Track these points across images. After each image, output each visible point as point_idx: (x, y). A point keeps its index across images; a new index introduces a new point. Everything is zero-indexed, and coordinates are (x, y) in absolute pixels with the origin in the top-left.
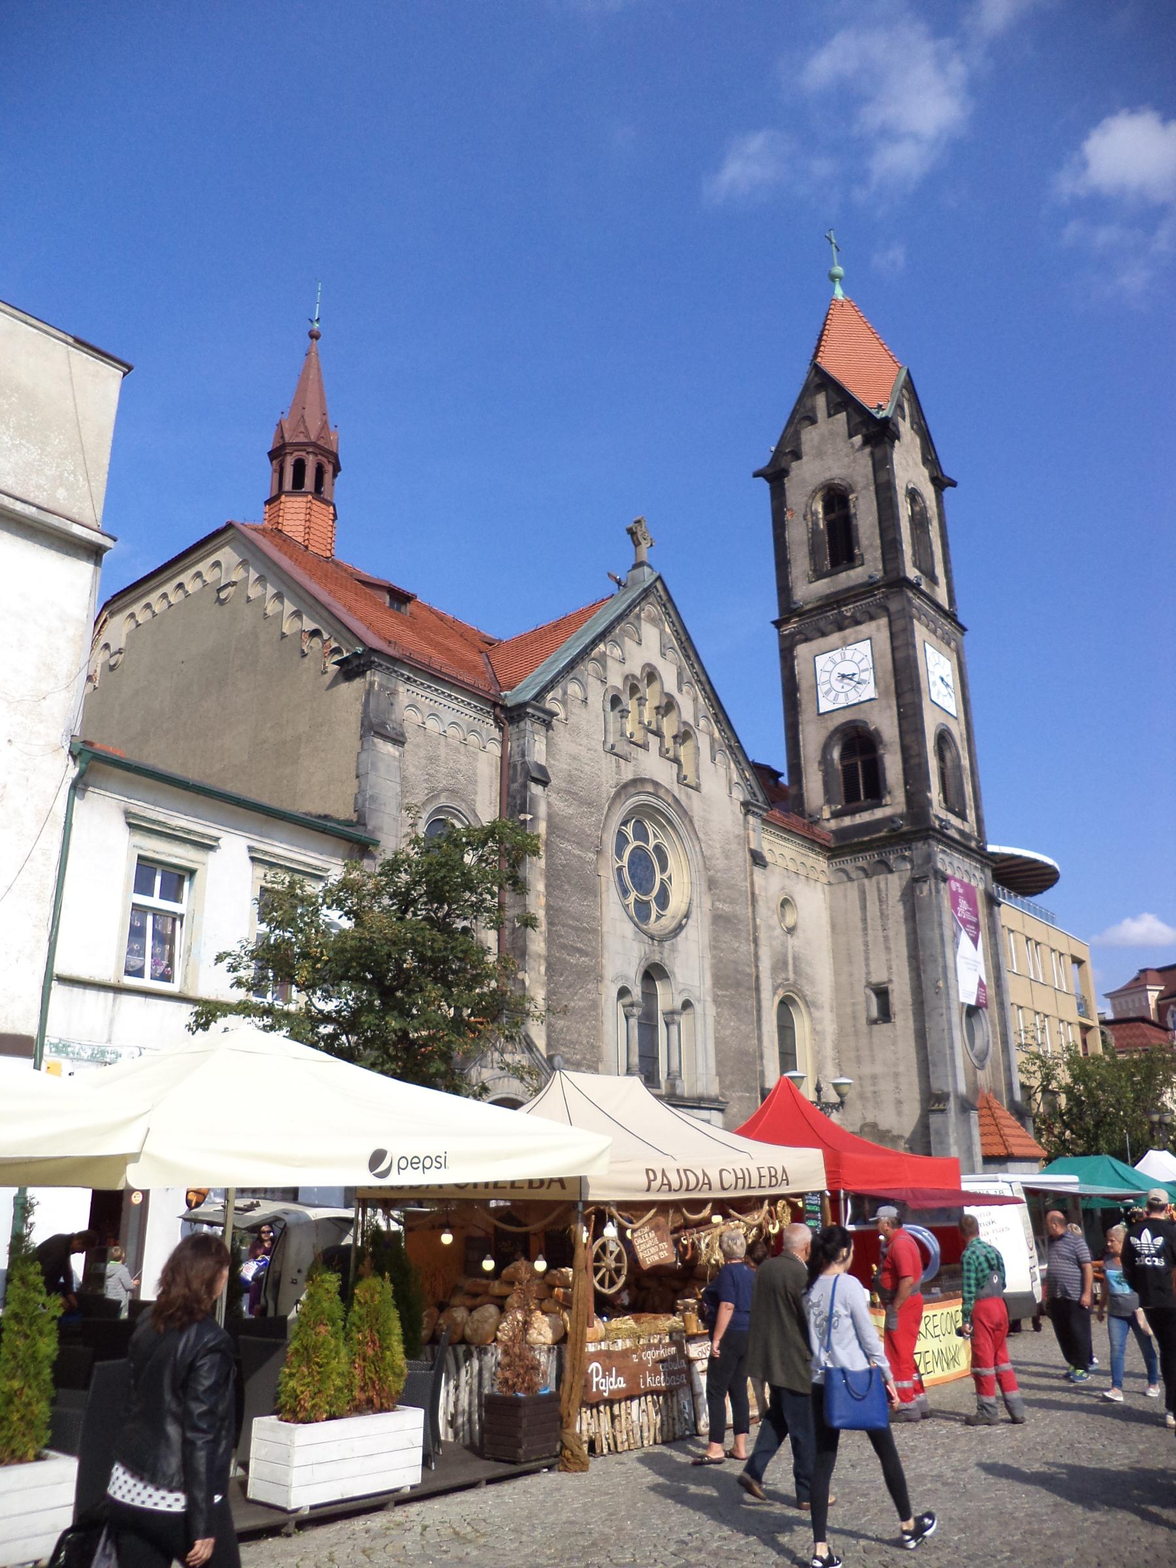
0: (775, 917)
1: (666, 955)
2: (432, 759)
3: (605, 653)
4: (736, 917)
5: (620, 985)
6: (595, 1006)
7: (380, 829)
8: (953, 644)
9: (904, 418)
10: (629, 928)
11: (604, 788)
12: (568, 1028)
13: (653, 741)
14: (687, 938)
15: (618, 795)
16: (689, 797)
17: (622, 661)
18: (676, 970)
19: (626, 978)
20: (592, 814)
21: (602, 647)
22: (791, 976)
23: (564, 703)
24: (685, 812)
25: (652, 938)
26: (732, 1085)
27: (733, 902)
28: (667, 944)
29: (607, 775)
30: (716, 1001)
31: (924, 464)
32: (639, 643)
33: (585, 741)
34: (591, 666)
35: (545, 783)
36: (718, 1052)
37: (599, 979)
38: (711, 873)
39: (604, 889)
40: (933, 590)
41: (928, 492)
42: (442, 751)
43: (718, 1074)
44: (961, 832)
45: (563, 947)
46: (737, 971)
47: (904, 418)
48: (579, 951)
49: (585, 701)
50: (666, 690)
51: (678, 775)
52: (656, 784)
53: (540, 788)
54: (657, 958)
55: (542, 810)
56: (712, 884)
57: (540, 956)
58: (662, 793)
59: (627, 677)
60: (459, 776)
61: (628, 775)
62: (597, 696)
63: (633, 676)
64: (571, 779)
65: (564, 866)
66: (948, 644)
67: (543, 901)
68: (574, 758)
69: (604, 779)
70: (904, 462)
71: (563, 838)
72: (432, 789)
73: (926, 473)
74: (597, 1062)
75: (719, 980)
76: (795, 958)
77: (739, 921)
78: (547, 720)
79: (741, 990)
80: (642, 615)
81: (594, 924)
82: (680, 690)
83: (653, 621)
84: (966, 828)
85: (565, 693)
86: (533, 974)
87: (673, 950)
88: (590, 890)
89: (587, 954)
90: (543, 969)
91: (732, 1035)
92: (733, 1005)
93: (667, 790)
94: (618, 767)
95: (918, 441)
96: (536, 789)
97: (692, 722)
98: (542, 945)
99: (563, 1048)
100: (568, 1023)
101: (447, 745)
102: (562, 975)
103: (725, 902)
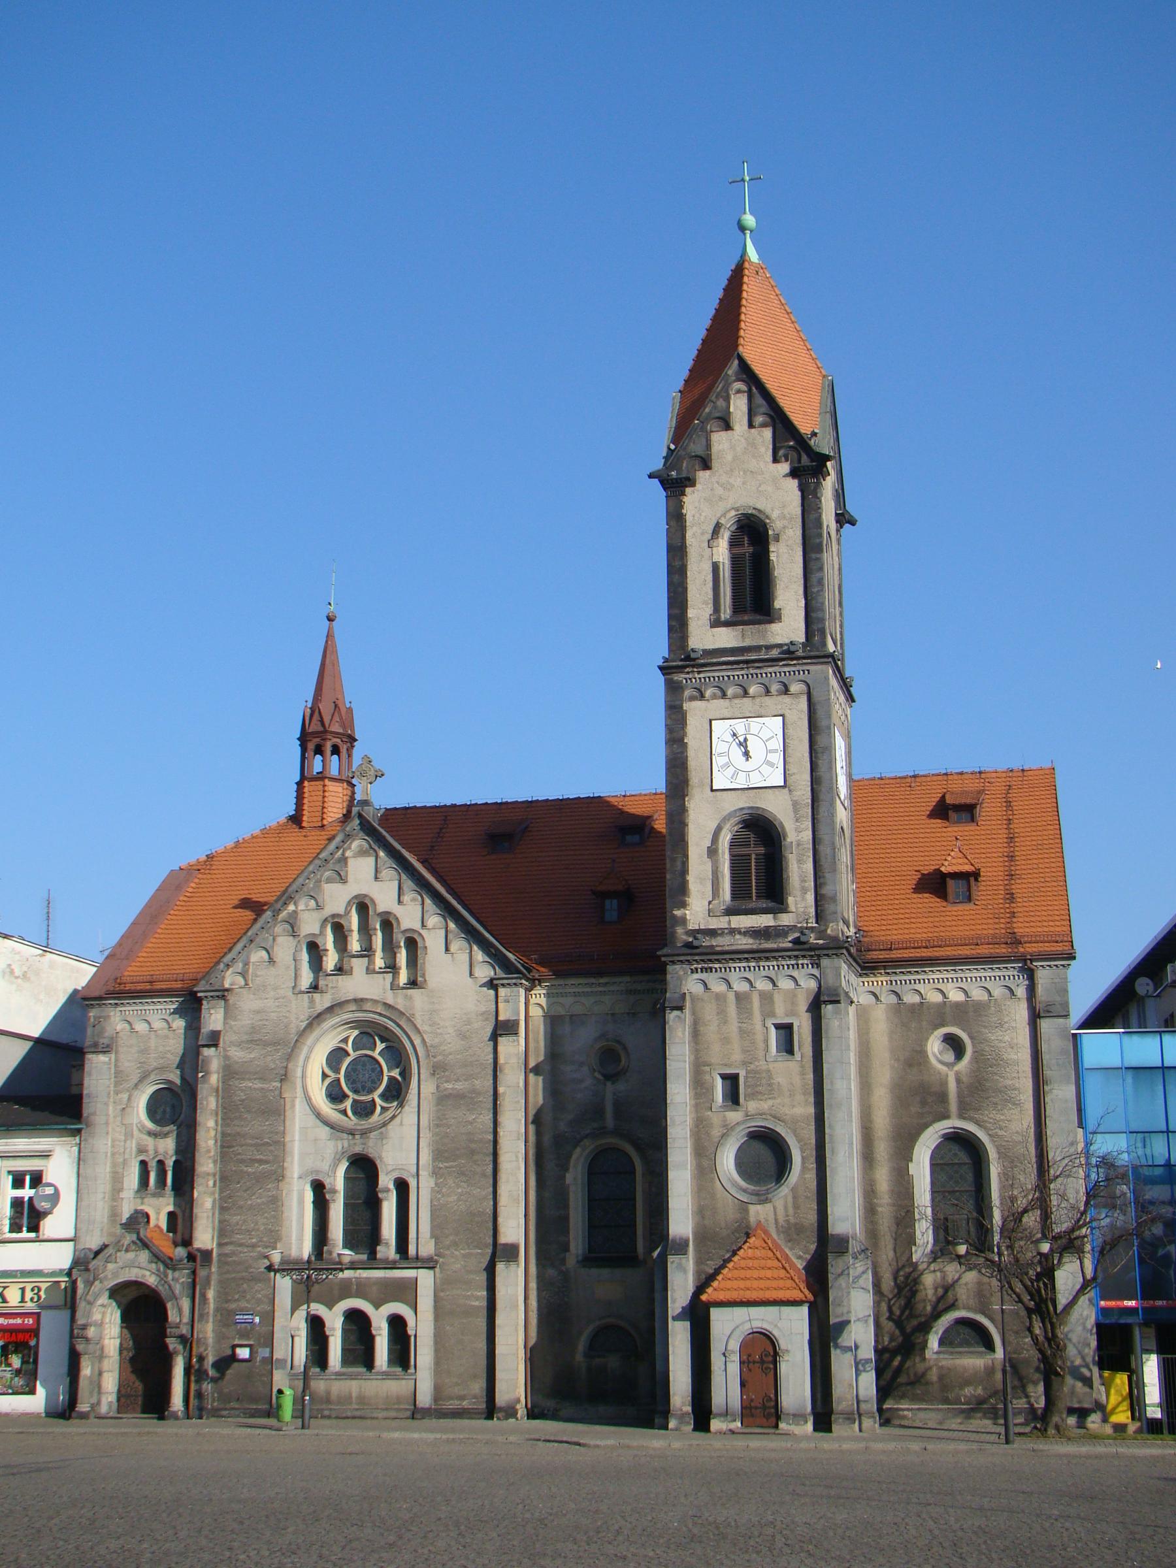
0: (585, 1069)
1: (371, 1143)
2: (144, 1051)
3: (295, 912)
4: (474, 1091)
5: (310, 1178)
6: (275, 1203)
7: (94, 1114)
8: (795, 688)
9: (727, 426)
10: (325, 1131)
11: (292, 1025)
12: (245, 1221)
13: (359, 965)
14: (401, 1124)
15: (310, 1026)
16: (411, 998)
17: (319, 907)
18: (384, 1155)
19: (317, 1172)
20: (277, 1051)
21: (291, 907)
22: (610, 1122)
23: (243, 974)
24: (402, 1014)
25: (352, 1133)
26: (455, 1244)
27: (468, 1078)
28: (372, 1135)
29: (300, 1010)
30: (436, 1173)
31: (775, 460)
32: (343, 880)
33: (272, 993)
34: (278, 929)
35: (216, 1045)
36: (433, 1220)
37: (279, 1176)
38: (440, 1058)
39: (287, 1108)
40: (764, 634)
41: (778, 497)
42: (153, 1043)
43: (432, 1237)
44: (756, 933)
45: (242, 1161)
46: (471, 1141)
47: (727, 426)
48: (260, 1162)
49: (271, 961)
50: (381, 908)
51: (392, 984)
52: (359, 1001)
53: (213, 1049)
54: (358, 1149)
55: (215, 1065)
56: (438, 1069)
57: (208, 1174)
58: (368, 1006)
59: (326, 920)
60: (169, 1056)
61: (322, 1001)
62: (287, 949)
63: (333, 916)
64: (254, 1030)
65: (243, 1101)
66: (786, 690)
67: (213, 1133)
68: (258, 1012)
69: (293, 1018)
70: (719, 491)
71: (243, 1079)
72: (144, 1072)
73: (785, 467)
74: (276, 1243)
75: (439, 1155)
76: (617, 1105)
77: (479, 1094)
78: (223, 994)
79: (476, 1157)
80: (348, 854)
81: (276, 1138)
82: (400, 902)
83: (362, 853)
84: (786, 920)
85: (246, 964)
87: (383, 1137)
88: (275, 1111)
89: (267, 1162)
90: (211, 1183)
91: (459, 1200)
92: (463, 1174)
93: (375, 1002)
94: (312, 1001)
95: (768, 433)
96: (208, 1052)
97: (417, 925)
98: (211, 1165)
101: (157, 1036)
103: (457, 1080)
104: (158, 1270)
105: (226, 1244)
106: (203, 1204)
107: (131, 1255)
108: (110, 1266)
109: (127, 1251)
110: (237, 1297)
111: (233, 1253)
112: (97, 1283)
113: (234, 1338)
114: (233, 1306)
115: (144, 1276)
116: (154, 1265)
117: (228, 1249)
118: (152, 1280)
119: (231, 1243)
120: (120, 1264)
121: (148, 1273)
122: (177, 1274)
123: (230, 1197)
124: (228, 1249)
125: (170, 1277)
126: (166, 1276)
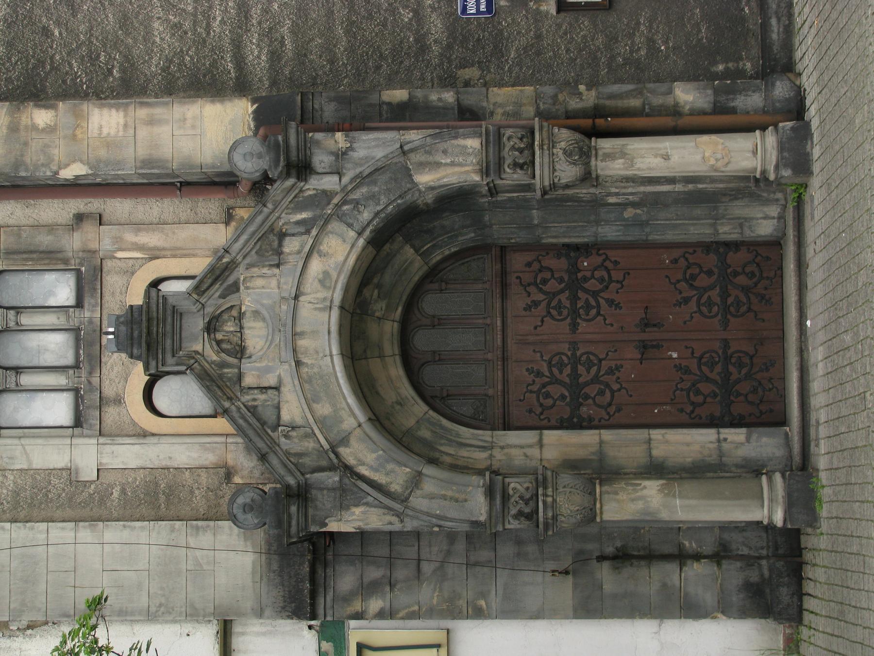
57: (14, 128)
86: (59, 152)
90: (42, 117)
99: (216, 24)
100: (158, 12)
102: (46, 32)
104: (306, 226)
105: (239, 61)
106: (109, 143)
107: (256, 336)
108: (292, 409)
109: (240, 352)
110: (407, 16)
111: (268, 34)
112: (348, 454)
113: (539, 17)
114: (436, 26)
115: (324, 280)
116: (291, 245)
117: (257, 55)
118: (339, 251)
119: (238, 46)
120: (285, 371)
121: (316, 266)
122: (321, 160)
123: (93, 58)
124: (257, 55)
125: (329, 183)
126: (327, 195)
